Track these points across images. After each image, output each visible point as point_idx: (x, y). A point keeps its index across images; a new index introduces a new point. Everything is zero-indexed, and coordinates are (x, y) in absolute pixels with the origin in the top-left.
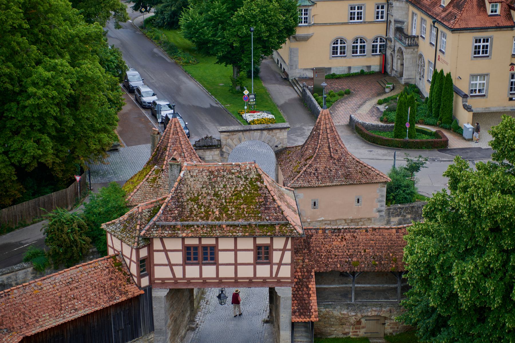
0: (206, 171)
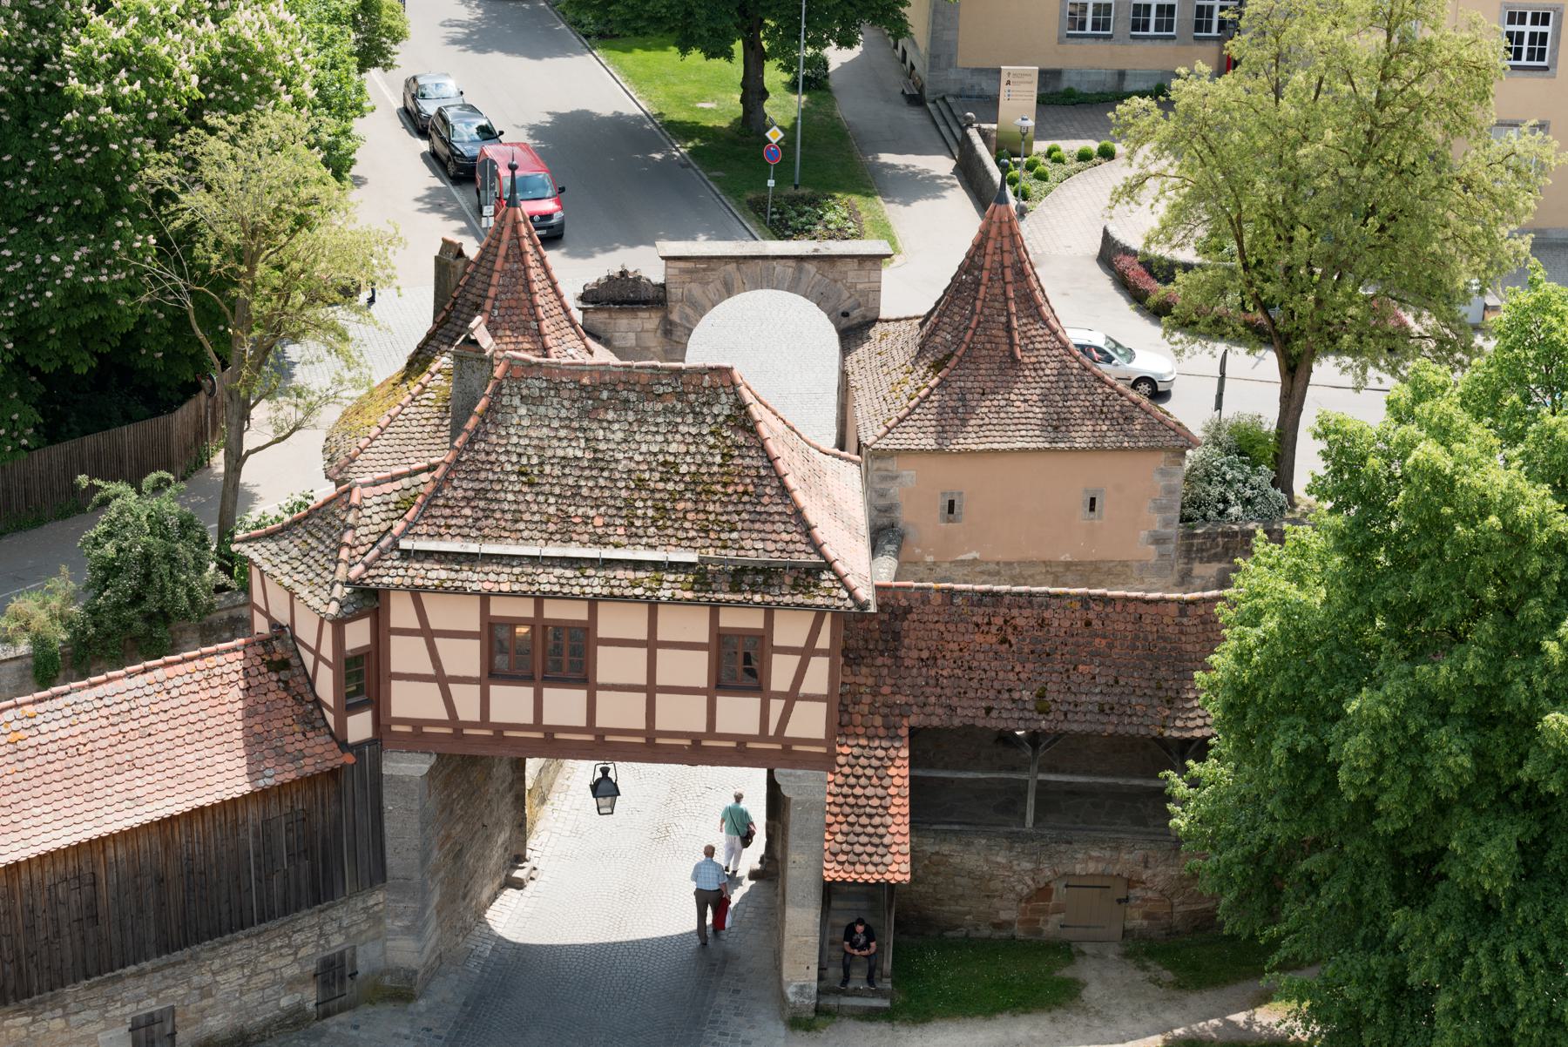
0: (572, 386)
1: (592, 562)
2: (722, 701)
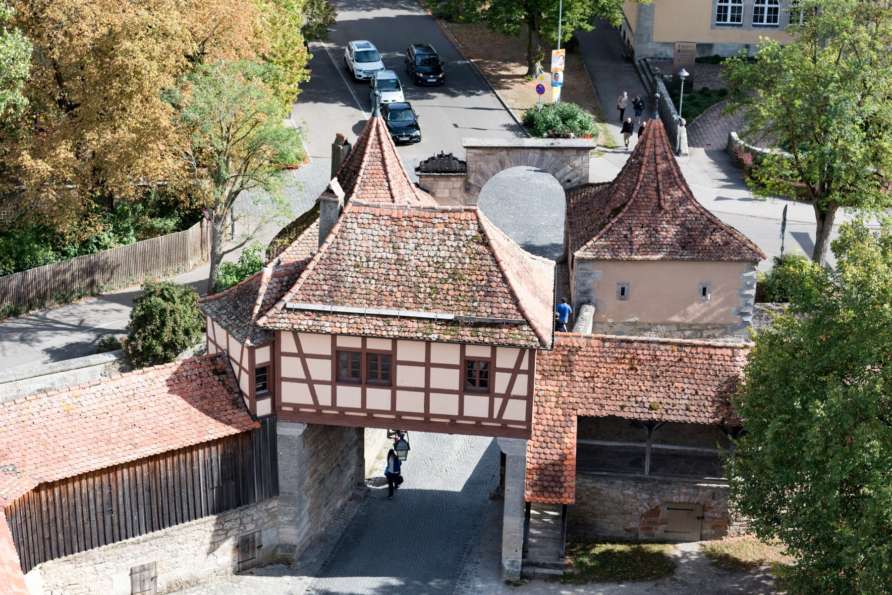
0: (386, 218)
1: (325, 313)
2: (340, 389)
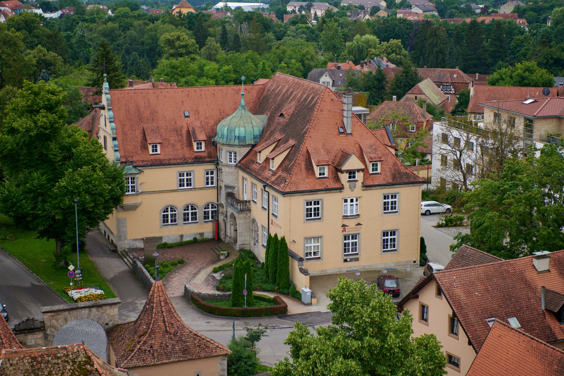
0: (28, 358)
